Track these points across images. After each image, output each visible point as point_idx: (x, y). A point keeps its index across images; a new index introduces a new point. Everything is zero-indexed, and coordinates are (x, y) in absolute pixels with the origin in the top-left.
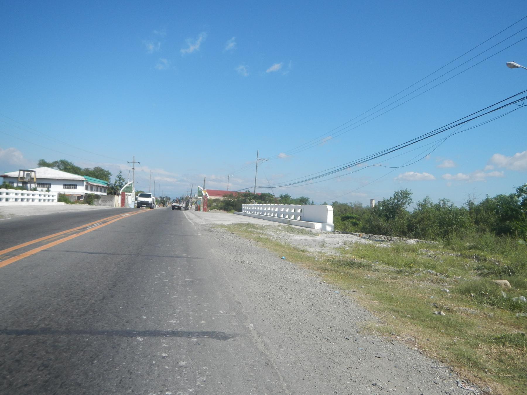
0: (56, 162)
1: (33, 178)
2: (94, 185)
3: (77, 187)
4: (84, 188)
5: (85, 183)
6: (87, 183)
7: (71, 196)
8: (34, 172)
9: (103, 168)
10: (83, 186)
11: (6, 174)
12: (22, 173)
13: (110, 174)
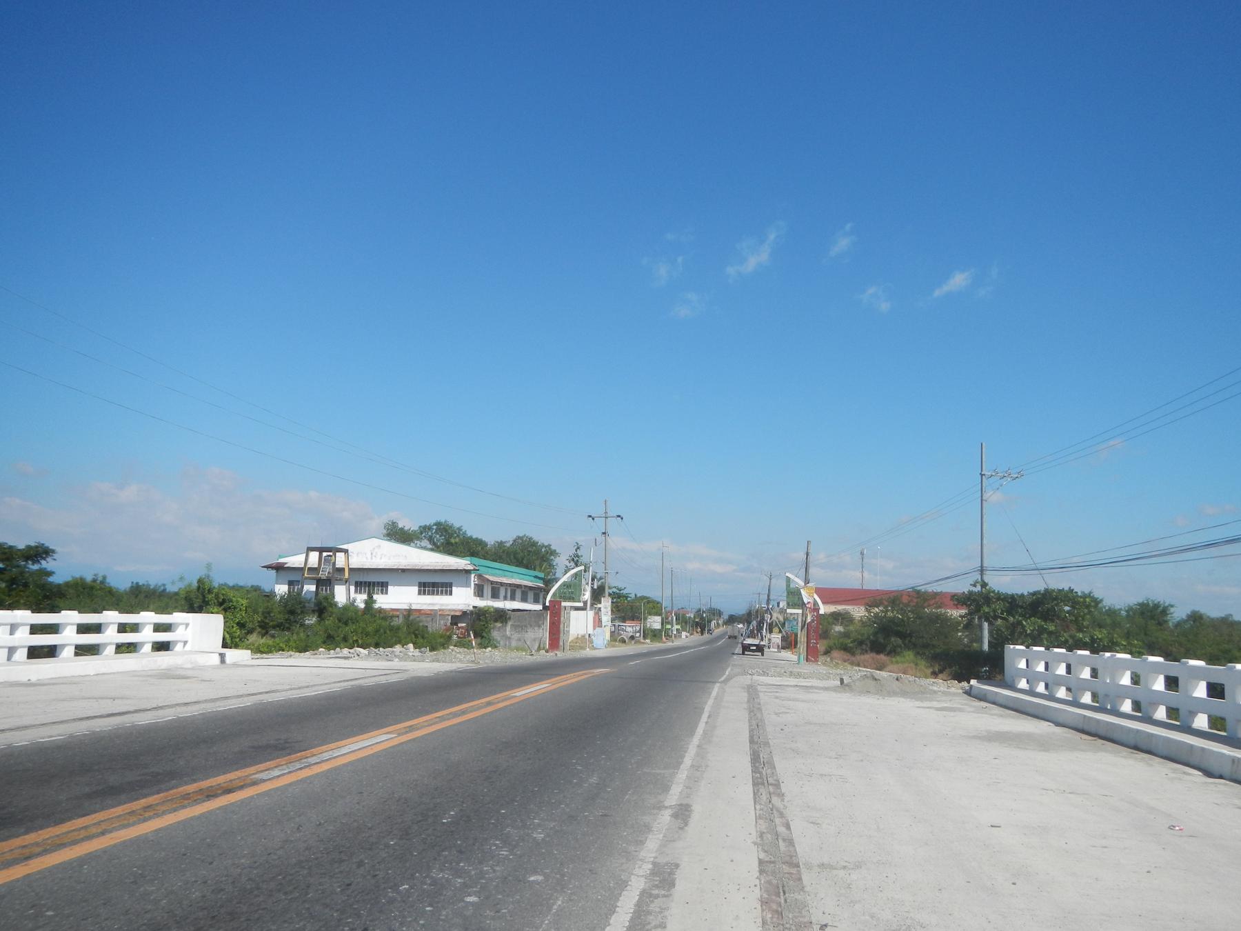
0: (425, 529)
1: (341, 570)
3: (454, 589)
4: (470, 591)
5: (473, 578)
6: (480, 576)
7: (432, 614)
8: (346, 551)
9: (536, 538)
10: (469, 586)
11: (281, 560)
12: (314, 558)
13: (554, 553)
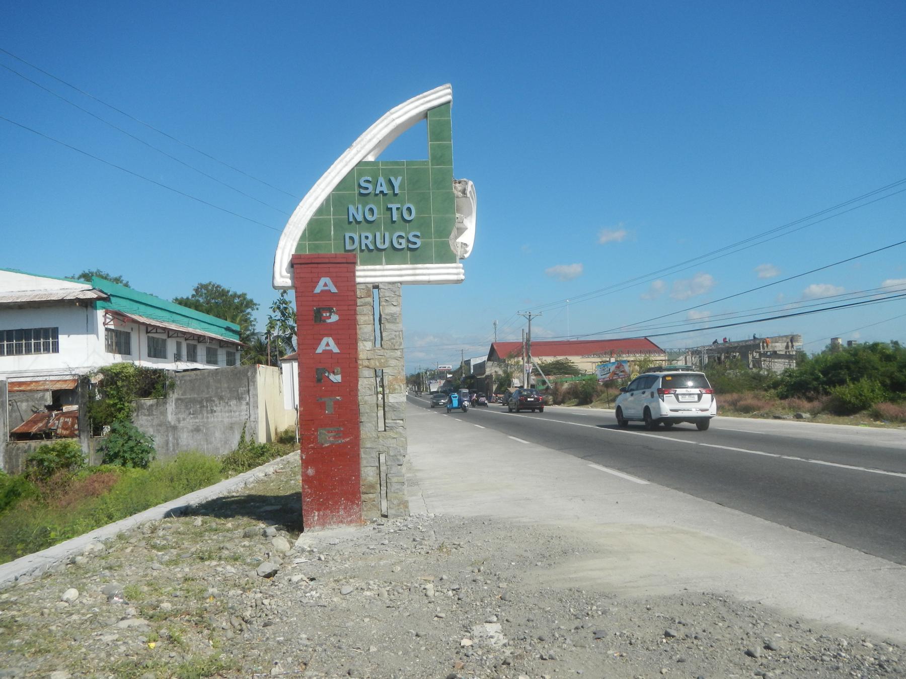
3: (62, 339)
6: (118, 315)
9: (225, 286)
13: (250, 304)
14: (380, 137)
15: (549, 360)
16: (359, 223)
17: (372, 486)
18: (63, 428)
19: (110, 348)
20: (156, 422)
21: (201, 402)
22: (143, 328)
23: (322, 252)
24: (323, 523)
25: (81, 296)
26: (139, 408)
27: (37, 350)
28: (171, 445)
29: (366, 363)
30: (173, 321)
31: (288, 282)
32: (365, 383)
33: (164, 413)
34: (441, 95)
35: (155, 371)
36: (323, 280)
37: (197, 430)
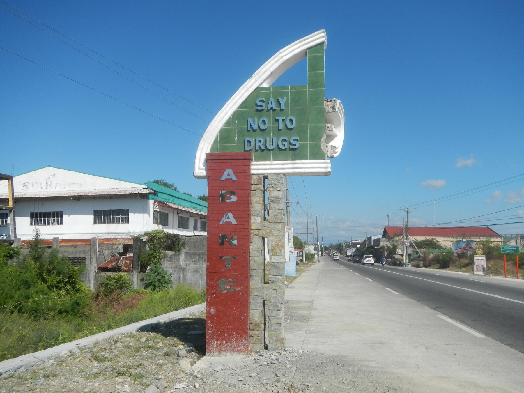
2: (191, 215)
3: (131, 215)
14: (272, 69)
15: (421, 238)
16: (255, 131)
17: (257, 325)
18: (125, 266)
19: (156, 222)
20: (174, 265)
21: (199, 255)
22: (176, 211)
23: (228, 151)
24: (220, 350)
25: (141, 192)
26: (165, 257)
27: (118, 222)
28: (181, 279)
29: (256, 232)
30: (193, 208)
31: (203, 173)
32: (254, 247)
33: (178, 260)
34: (318, 37)
35: (175, 236)
36: (227, 172)
37: (196, 271)
